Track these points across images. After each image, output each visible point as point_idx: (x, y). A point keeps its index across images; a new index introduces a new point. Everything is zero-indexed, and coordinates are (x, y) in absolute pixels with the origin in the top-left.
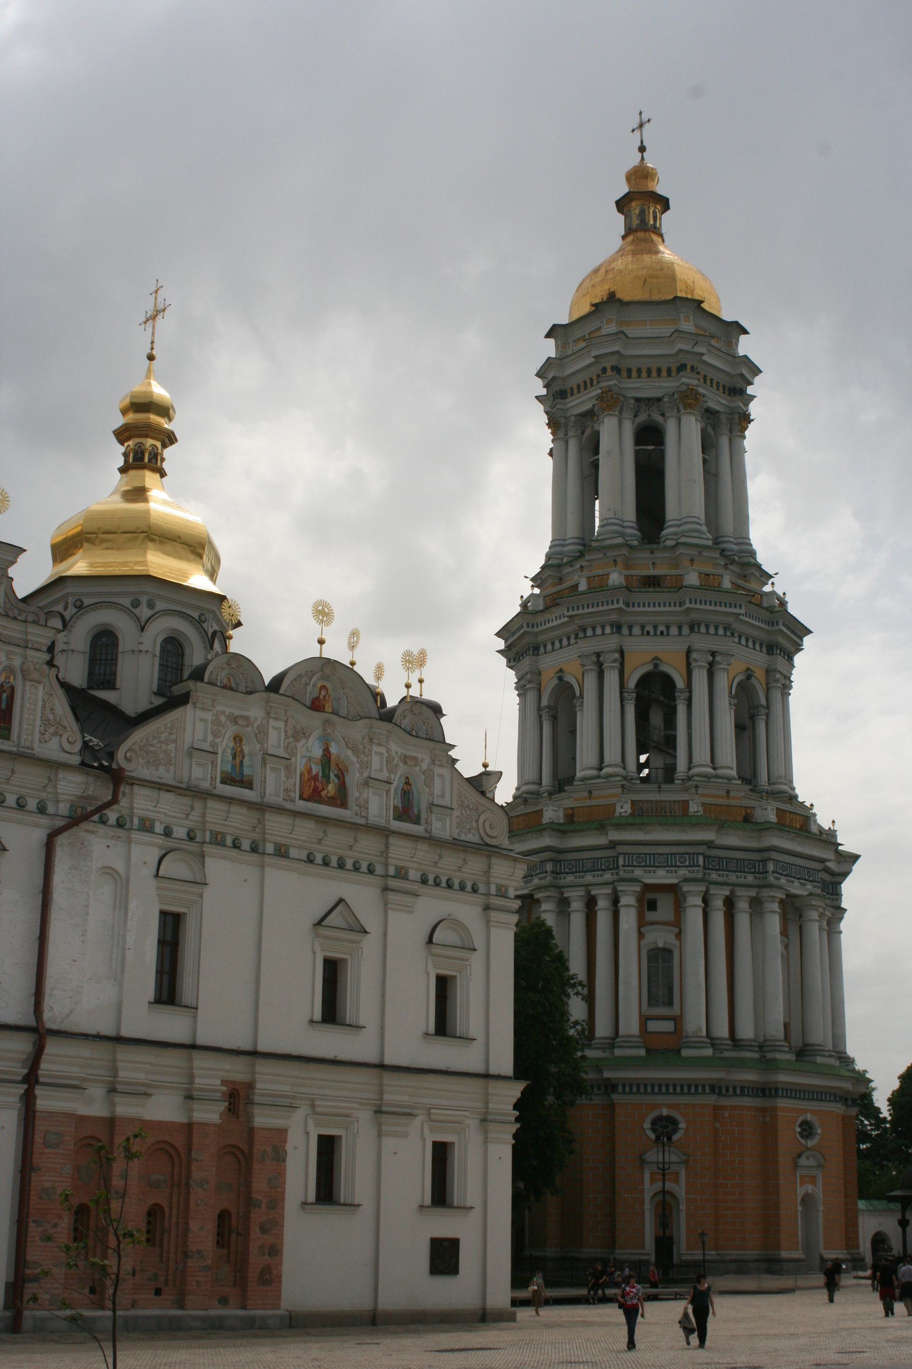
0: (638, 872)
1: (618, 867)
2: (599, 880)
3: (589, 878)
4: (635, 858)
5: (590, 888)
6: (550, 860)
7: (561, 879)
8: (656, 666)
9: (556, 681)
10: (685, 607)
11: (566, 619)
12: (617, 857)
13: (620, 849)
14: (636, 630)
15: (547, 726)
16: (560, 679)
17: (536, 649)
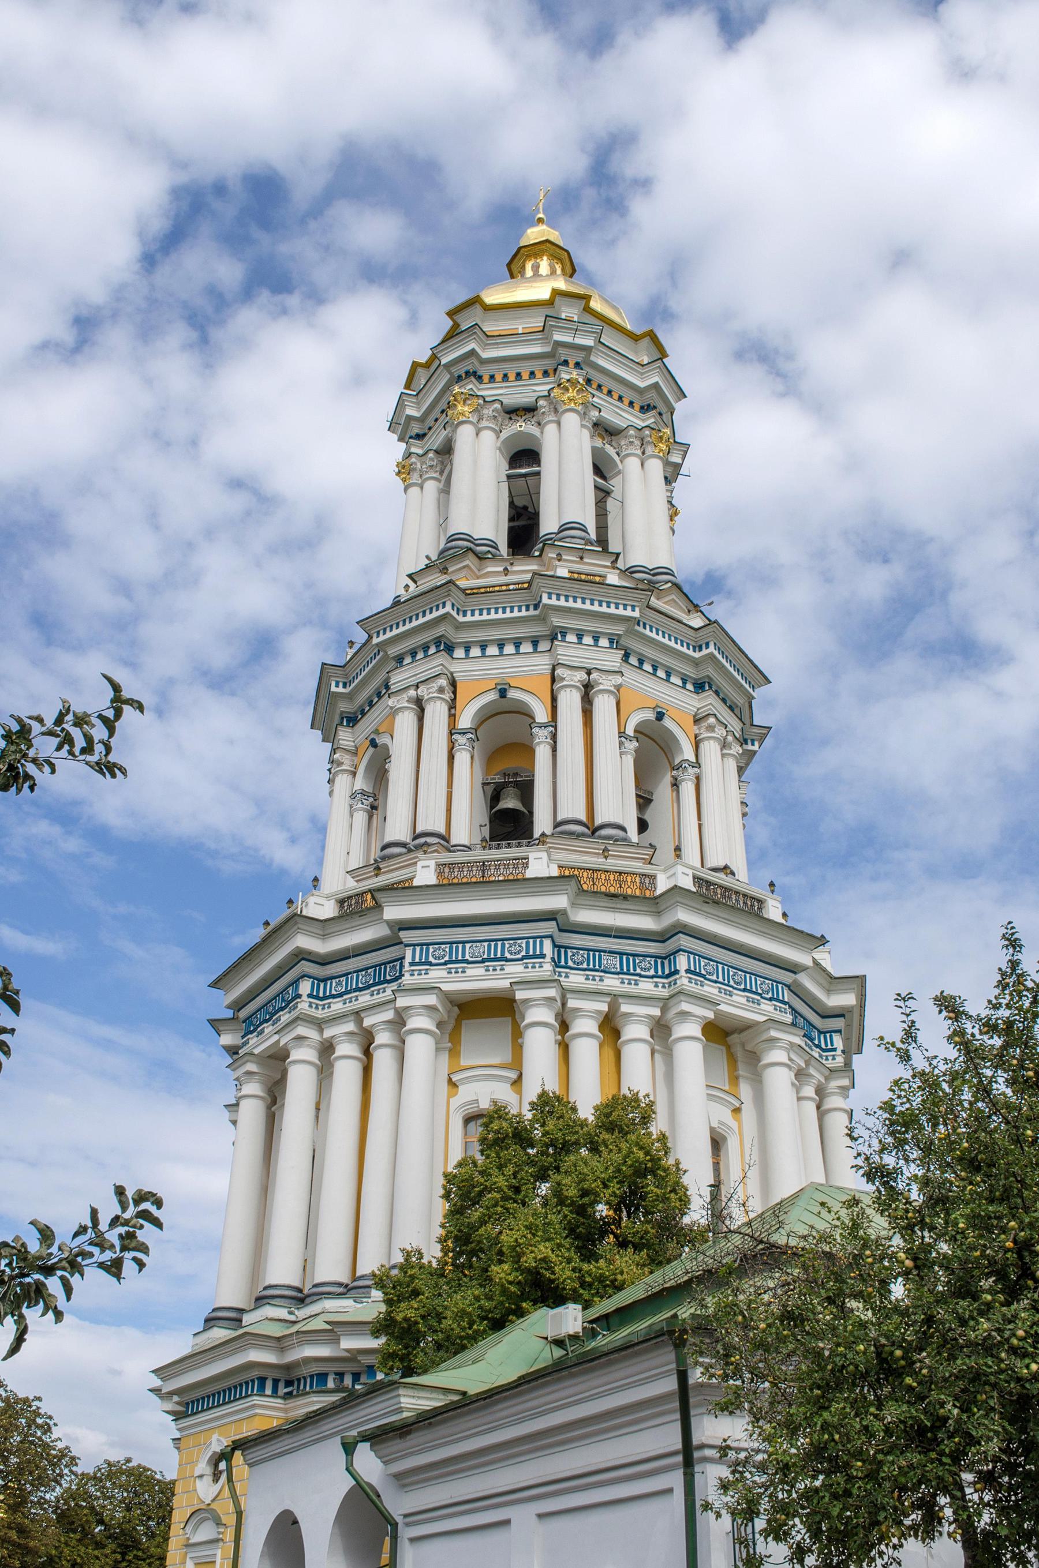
0: (710, 990)
1: (676, 972)
2: (632, 989)
3: (612, 983)
4: (702, 964)
5: (620, 1000)
6: (551, 937)
7: (560, 975)
8: (660, 716)
9: (493, 696)
10: (705, 652)
11: (532, 612)
12: (670, 956)
13: (684, 941)
14: (633, 660)
15: (463, 758)
16: (503, 693)
17: (450, 649)
